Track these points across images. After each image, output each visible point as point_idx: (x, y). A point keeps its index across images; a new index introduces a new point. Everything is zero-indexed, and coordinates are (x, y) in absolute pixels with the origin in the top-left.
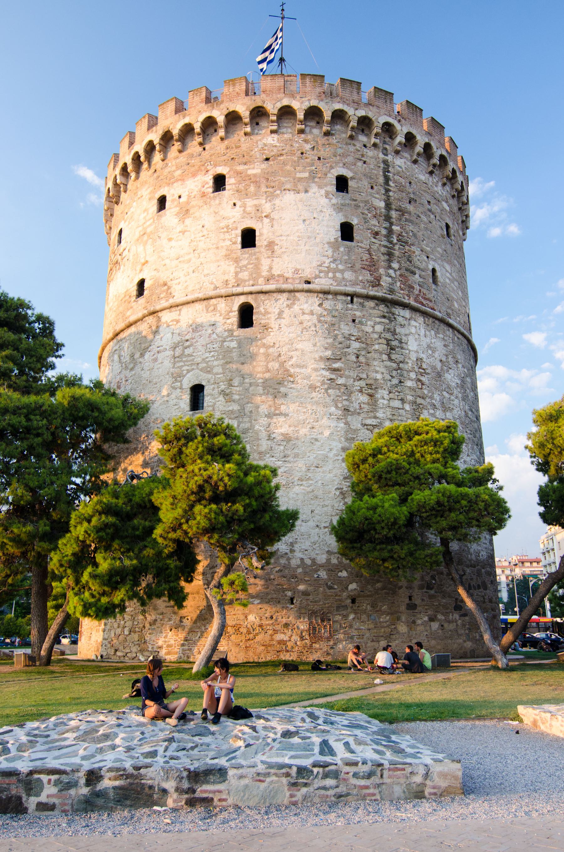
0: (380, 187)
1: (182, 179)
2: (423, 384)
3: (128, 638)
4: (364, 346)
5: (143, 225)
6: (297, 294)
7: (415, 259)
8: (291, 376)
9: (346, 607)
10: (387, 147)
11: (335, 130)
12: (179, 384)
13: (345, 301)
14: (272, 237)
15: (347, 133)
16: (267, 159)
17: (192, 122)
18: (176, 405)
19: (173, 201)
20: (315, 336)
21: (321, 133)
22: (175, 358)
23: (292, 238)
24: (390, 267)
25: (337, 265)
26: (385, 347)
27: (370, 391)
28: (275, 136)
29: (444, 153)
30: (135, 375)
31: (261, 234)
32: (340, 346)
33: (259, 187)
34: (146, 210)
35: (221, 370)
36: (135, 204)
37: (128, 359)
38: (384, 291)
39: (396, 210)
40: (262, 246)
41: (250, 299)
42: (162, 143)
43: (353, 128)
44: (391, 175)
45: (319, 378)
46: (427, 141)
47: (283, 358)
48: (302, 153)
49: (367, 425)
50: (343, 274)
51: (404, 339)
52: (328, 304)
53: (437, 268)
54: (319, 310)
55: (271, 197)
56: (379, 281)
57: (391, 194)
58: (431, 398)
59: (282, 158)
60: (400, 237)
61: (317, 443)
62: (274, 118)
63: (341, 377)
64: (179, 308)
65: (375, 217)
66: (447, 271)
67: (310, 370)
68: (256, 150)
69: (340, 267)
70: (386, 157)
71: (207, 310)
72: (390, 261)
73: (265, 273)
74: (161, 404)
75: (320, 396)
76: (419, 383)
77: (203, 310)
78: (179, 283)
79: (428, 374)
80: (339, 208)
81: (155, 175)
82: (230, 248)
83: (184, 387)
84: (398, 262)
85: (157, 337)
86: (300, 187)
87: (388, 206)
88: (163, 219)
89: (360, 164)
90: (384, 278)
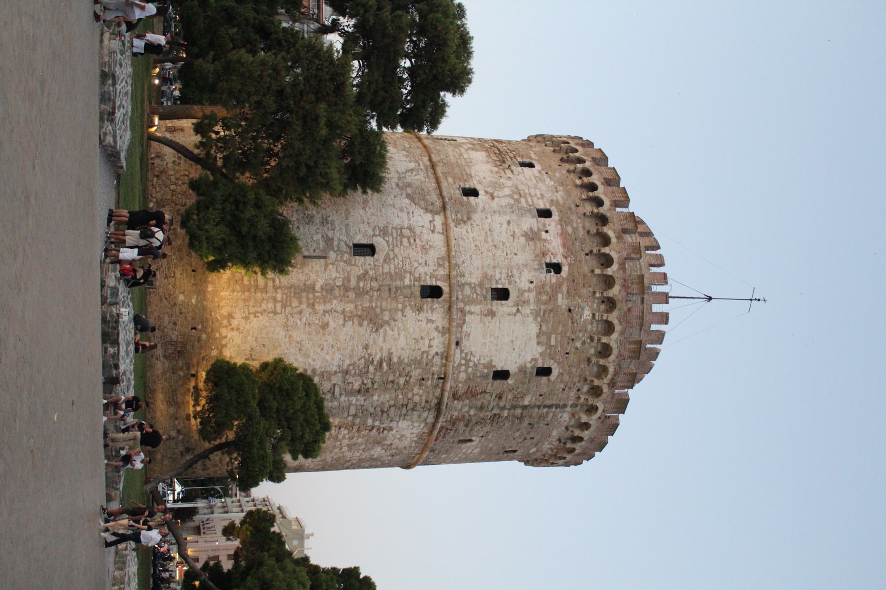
0: (542, 401)
1: (563, 234)
2: (370, 430)
3: (167, 189)
4: (402, 386)
5: (530, 194)
6: (447, 335)
7: (478, 427)
9: (188, 369)
10: (579, 408)
11: (593, 366)
12: (377, 233)
15: (590, 375)
16: (570, 310)
17: (610, 246)
18: (359, 230)
19: (544, 225)
20: (410, 349)
21: (591, 355)
22: (401, 229)
24: (470, 408)
25: (471, 367)
26: (401, 403)
27: (363, 391)
28: (590, 318)
29: (577, 451)
30: (392, 188)
31: (502, 305)
32: (401, 369)
33: (545, 304)
34: (542, 195)
35: (385, 271)
36: (552, 183)
37: (409, 180)
38: (449, 404)
39: (522, 414)
40: (492, 306)
41: (445, 296)
42: (599, 214)
43: (592, 381)
44: (554, 409)
46: (585, 439)
48: (573, 340)
49: (334, 388)
50: (464, 371)
51: (409, 418)
52: (437, 360)
53: (473, 443)
54: (433, 352)
55: (536, 314)
56: (458, 399)
58: (358, 437)
60: (497, 416)
61: (320, 349)
63: (375, 369)
64: (445, 233)
66: (473, 450)
67: (381, 344)
68: (579, 301)
69: (470, 370)
70: (569, 406)
71: (440, 258)
72: (476, 408)
73: (467, 308)
74: (361, 216)
75: (359, 352)
76: (370, 428)
77: (440, 254)
78: (467, 232)
79: (379, 433)
80: (522, 370)
81: (573, 206)
82: (493, 278)
83: (374, 238)
85: (422, 211)
86: (543, 339)
87: (524, 407)
88: (528, 215)
89: (562, 386)
90: (461, 403)
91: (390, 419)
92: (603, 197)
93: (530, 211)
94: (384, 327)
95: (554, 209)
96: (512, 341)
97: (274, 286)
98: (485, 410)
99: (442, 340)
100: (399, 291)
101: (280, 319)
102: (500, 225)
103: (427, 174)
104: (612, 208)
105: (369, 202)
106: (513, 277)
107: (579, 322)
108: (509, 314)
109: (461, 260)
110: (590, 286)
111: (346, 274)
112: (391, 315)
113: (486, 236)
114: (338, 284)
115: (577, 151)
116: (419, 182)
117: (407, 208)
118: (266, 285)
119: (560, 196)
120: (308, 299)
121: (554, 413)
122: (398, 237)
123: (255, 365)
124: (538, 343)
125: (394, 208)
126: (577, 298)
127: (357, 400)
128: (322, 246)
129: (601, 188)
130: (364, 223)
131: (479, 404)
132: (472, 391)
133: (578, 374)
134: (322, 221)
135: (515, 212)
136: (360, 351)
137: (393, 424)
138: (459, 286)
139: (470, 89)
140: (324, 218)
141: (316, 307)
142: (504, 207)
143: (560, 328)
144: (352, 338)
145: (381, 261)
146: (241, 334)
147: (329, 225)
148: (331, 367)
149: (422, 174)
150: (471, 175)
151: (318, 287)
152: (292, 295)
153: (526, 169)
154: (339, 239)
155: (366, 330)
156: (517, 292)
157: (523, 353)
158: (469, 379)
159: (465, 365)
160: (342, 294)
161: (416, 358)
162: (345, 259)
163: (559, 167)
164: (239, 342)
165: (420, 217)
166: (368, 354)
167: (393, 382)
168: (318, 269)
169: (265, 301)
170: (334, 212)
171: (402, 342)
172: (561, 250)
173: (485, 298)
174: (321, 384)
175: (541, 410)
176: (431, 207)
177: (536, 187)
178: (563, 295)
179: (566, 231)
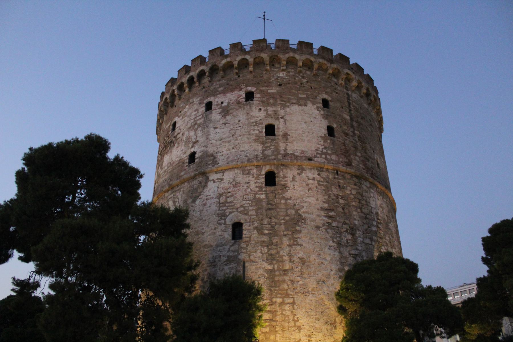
1: (224, 92)
5: (194, 119)
7: (368, 152)
8: (303, 219)
12: (223, 221)
13: (334, 173)
14: (286, 130)
16: (280, 85)
17: (232, 61)
18: (221, 235)
19: (217, 105)
23: (298, 132)
25: (327, 151)
26: (358, 204)
28: (285, 73)
31: (279, 128)
35: (254, 213)
36: (187, 106)
40: (279, 135)
41: (273, 169)
44: (351, 102)
45: (321, 222)
47: (297, 207)
48: (301, 84)
50: (331, 156)
51: (368, 200)
52: (324, 174)
55: (284, 106)
56: (351, 163)
57: (352, 112)
59: (289, 85)
62: (285, 63)
65: (346, 124)
67: (315, 216)
73: (282, 152)
75: (322, 234)
77: (240, 173)
80: (325, 117)
81: (204, 90)
82: (258, 135)
83: (227, 223)
84: (360, 152)
86: (302, 102)
87: (352, 119)
88: (210, 116)
89: (334, 93)
90: (353, 161)
91: (370, 213)
92: (197, 71)
93: (206, 116)
94: (300, 213)
95: (205, 102)
96: (305, 122)
97: (270, 305)
98: (356, 145)
99: (308, 171)
100: (271, 202)
101: (298, 298)
102: (217, 134)
103: (177, 190)
104: (206, 64)
105: (198, 230)
106: (257, 122)
107: (288, 80)
108: (285, 124)
109: (244, 157)
110: (262, 73)
111: (258, 244)
112: (291, 208)
113: (226, 142)
114: (266, 251)
115: (166, 98)
116: (183, 195)
117: (203, 201)
118: (269, 312)
119: (196, 100)
120: (280, 275)
121: (353, 102)
122: (227, 205)
123: (339, 319)
124: (306, 105)
125: (203, 210)
126: (271, 81)
127: (360, 237)
128: (234, 265)
129: (192, 74)
130: (214, 233)
131: (353, 149)
132: (345, 153)
133: (325, 83)
134: (213, 266)
135: (207, 125)
136: (321, 233)
137: (374, 211)
138: (265, 158)
139: (104, 135)
140: (211, 264)
141: (287, 268)
142: (203, 133)
143: (294, 91)
144: (311, 239)
145: (247, 217)
146: (314, 333)
147: (217, 260)
148: (336, 256)
149: (177, 194)
150: (179, 160)
151: (270, 267)
152: (277, 289)
153: (177, 126)
154: (228, 251)
155: (303, 227)
156: (268, 119)
157: (314, 116)
158: (336, 153)
159: (326, 155)
160: (275, 247)
161: (324, 190)
162: (245, 246)
163: (177, 107)
164: (321, 335)
165: (210, 191)
166: (323, 226)
167: (343, 209)
168: (254, 267)
169: (284, 313)
170: (206, 257)
171: (312, 200)
172: (236, 93)
173: (273, 140)
174: (350, 264)
175: (352, 110)
176: (203, 184)
177: (190, 116)
178: (269, 89)
179: (222, 91)
